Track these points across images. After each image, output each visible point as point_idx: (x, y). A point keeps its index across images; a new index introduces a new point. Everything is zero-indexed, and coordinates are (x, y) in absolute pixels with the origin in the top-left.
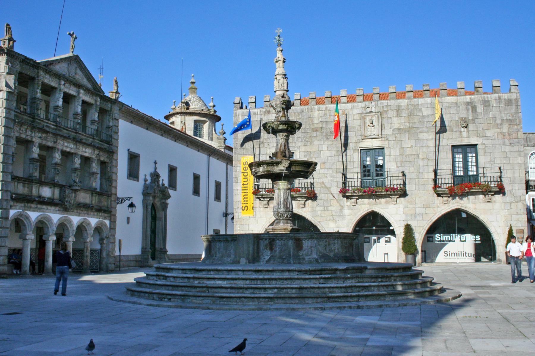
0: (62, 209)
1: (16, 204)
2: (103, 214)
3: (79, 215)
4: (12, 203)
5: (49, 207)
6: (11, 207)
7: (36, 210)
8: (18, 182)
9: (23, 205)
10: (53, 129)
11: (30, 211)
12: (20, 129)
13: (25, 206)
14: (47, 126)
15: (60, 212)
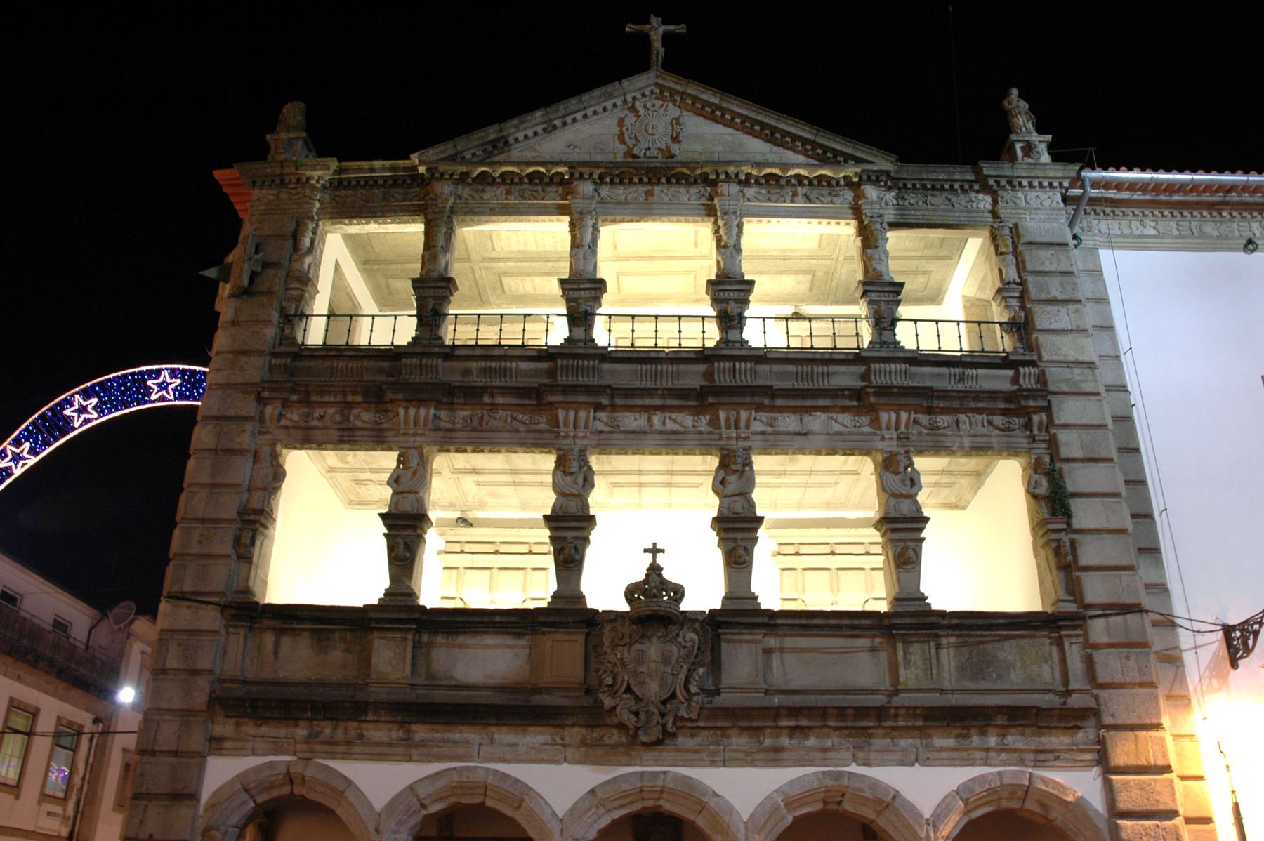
0: (615, 737)
1: (249, 729)
2: (1013, 740)
3: (775, 757)
4: (223, 728)
5: (505, 736)
6: (216, 745)
7: (407, 750)
8: (280, 632)
9: (301, 732)
10: (536, 373)
11: (347, 756)
12: (307, 416)
13: (312, 738)
14: (486, 371)
15: (591, 753)
